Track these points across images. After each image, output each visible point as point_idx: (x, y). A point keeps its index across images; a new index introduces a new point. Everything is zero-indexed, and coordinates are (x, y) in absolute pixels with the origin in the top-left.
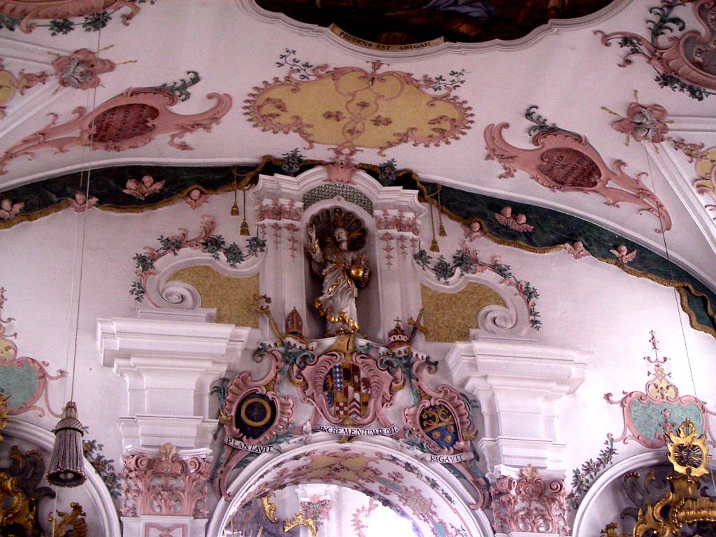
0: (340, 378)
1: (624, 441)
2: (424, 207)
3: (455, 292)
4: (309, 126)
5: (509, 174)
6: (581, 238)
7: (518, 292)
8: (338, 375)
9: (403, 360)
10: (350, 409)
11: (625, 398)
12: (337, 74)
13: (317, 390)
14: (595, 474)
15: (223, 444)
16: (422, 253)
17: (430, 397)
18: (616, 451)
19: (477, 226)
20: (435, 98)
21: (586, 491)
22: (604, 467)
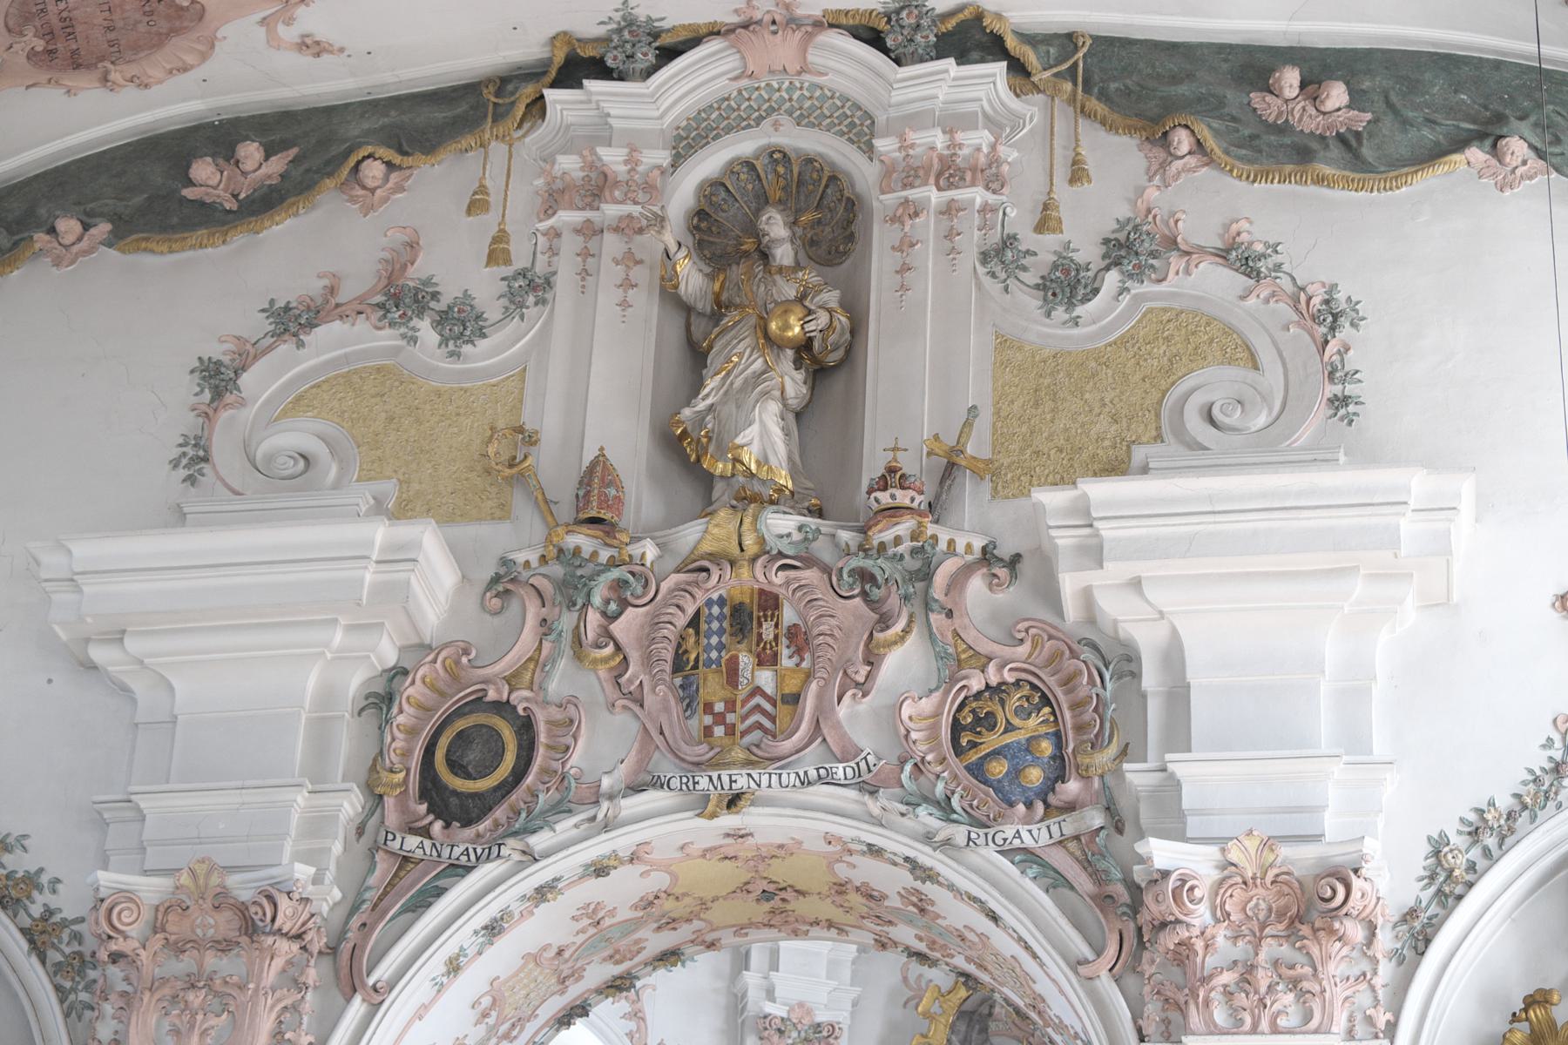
0: (721, 632)
2: (1031, 109)
6: (1525, 127)
7: (1295, 317)
10: (744, 718)
15: (374, 849)
16: (1009, 241)
17: (983, 660)
22: (1533, 818)
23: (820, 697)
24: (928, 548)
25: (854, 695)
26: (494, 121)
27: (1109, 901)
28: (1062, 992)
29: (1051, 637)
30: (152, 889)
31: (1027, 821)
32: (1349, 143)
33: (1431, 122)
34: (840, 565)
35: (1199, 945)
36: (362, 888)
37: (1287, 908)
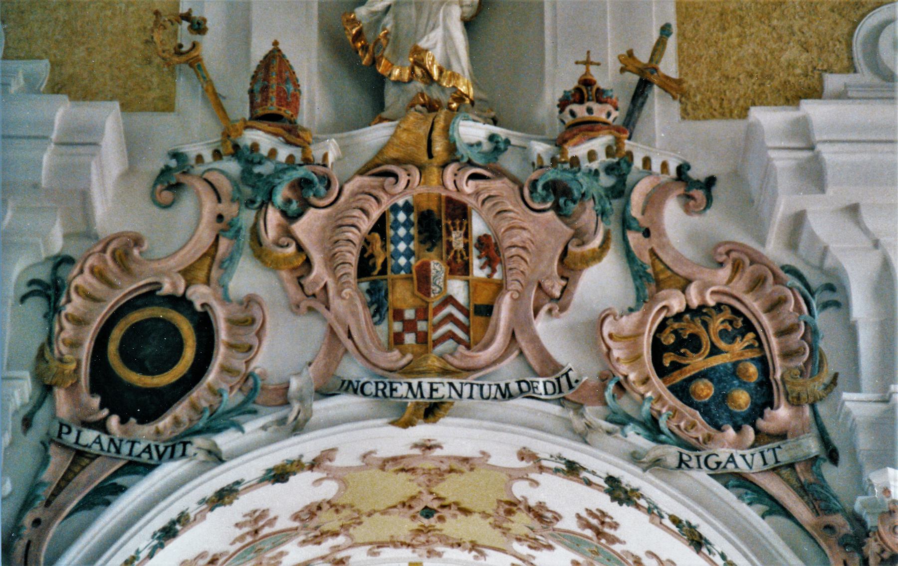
0: (408, 239)
8: (402, 232)
9: (602, 175)
13: (338, 279)
24: (624, 166)
25: (550, 311)
29: (752, 262)
31: (738, 445)
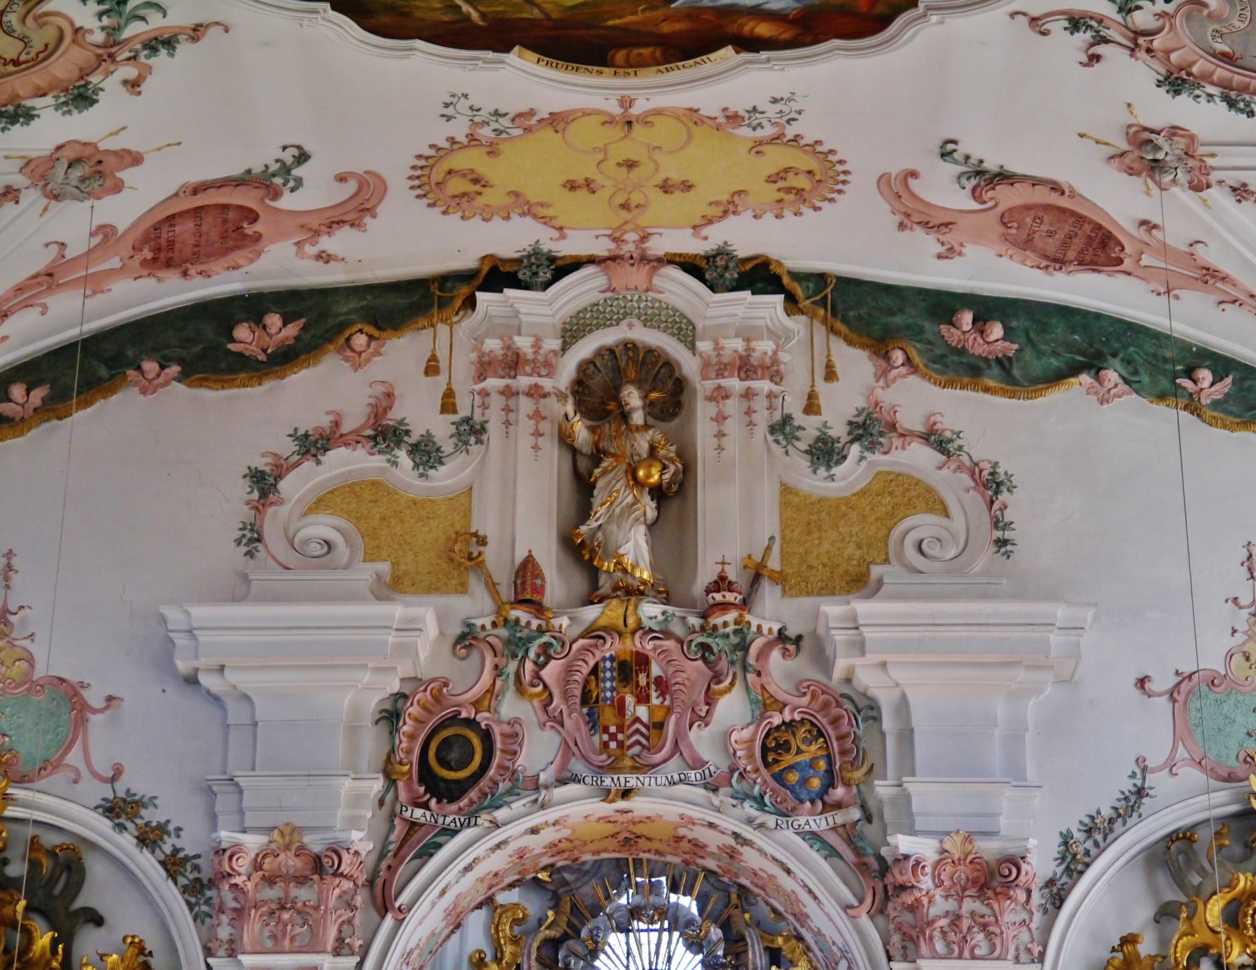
0: (612, 679)
1: (1171, 770)
2: (798, 324)
3: (848, 494)
4: (542, 205)
5: (949, 253)
6: (1116, 362)
7: (973, 484)
8: (608, 674)
9: (732, 636)
10: (629, 737)
11: (1179, 684)
12: (557, 121)
13: (569, 707)
14: (1105, 839)
15: (392, 816)
16: (787, 419)
18: (1151, 792)
19: (898, 356)
20: (760, 143)
21: (1081, 873)
22: (1124, 823)
23: (677, 724)
24: (745, 630)
25: (699, 725)
26: (439, 308)
27: (864, 867)
28: (830, 919)
29: (823, 692)
30: (253, 842)
31: (812, 814)
32: (1004, 364)
33: (1055, 354)
34: (689, 638)
35: (925, 901)
36: (385, 842)
37: (978, 877)
